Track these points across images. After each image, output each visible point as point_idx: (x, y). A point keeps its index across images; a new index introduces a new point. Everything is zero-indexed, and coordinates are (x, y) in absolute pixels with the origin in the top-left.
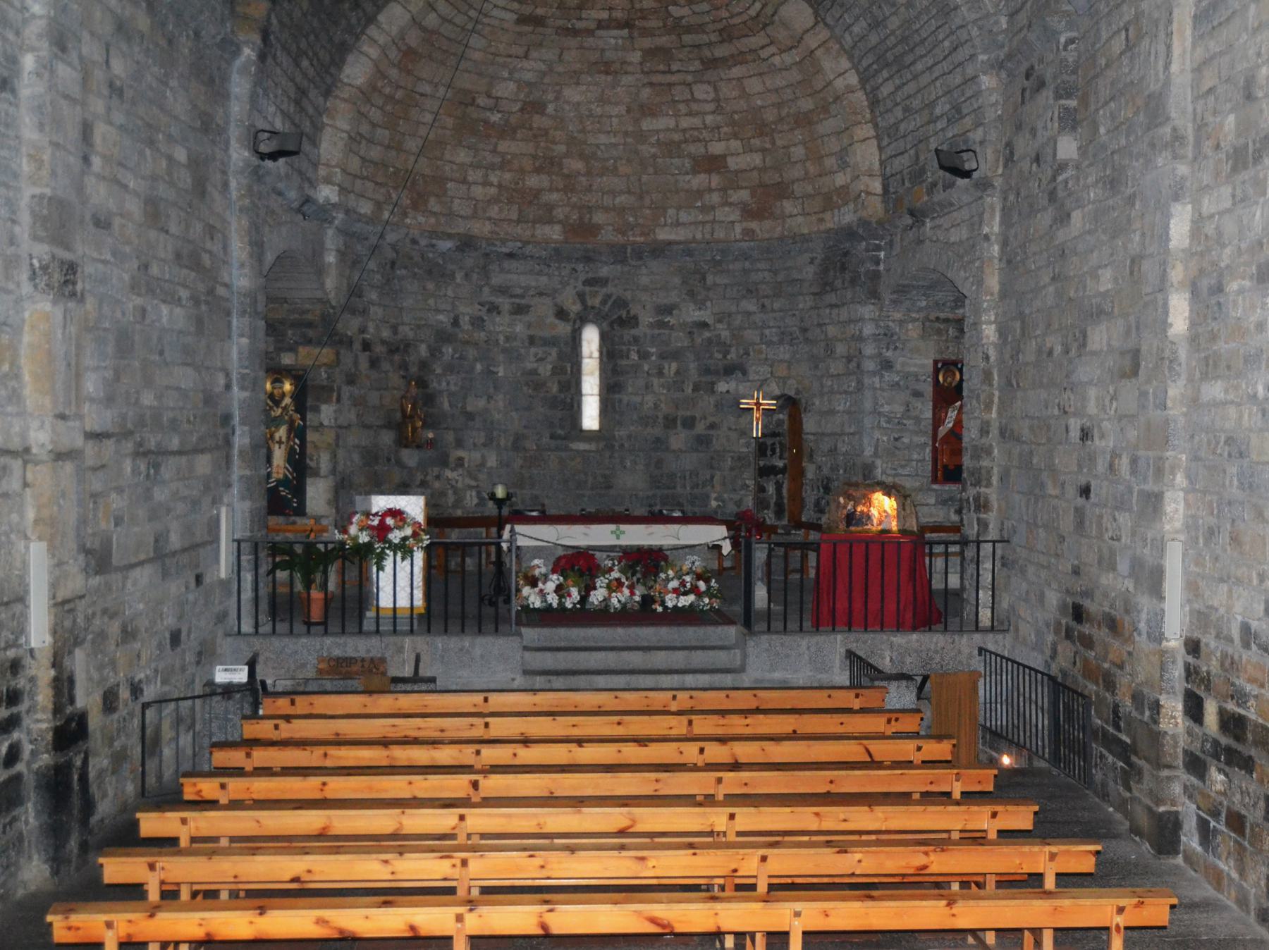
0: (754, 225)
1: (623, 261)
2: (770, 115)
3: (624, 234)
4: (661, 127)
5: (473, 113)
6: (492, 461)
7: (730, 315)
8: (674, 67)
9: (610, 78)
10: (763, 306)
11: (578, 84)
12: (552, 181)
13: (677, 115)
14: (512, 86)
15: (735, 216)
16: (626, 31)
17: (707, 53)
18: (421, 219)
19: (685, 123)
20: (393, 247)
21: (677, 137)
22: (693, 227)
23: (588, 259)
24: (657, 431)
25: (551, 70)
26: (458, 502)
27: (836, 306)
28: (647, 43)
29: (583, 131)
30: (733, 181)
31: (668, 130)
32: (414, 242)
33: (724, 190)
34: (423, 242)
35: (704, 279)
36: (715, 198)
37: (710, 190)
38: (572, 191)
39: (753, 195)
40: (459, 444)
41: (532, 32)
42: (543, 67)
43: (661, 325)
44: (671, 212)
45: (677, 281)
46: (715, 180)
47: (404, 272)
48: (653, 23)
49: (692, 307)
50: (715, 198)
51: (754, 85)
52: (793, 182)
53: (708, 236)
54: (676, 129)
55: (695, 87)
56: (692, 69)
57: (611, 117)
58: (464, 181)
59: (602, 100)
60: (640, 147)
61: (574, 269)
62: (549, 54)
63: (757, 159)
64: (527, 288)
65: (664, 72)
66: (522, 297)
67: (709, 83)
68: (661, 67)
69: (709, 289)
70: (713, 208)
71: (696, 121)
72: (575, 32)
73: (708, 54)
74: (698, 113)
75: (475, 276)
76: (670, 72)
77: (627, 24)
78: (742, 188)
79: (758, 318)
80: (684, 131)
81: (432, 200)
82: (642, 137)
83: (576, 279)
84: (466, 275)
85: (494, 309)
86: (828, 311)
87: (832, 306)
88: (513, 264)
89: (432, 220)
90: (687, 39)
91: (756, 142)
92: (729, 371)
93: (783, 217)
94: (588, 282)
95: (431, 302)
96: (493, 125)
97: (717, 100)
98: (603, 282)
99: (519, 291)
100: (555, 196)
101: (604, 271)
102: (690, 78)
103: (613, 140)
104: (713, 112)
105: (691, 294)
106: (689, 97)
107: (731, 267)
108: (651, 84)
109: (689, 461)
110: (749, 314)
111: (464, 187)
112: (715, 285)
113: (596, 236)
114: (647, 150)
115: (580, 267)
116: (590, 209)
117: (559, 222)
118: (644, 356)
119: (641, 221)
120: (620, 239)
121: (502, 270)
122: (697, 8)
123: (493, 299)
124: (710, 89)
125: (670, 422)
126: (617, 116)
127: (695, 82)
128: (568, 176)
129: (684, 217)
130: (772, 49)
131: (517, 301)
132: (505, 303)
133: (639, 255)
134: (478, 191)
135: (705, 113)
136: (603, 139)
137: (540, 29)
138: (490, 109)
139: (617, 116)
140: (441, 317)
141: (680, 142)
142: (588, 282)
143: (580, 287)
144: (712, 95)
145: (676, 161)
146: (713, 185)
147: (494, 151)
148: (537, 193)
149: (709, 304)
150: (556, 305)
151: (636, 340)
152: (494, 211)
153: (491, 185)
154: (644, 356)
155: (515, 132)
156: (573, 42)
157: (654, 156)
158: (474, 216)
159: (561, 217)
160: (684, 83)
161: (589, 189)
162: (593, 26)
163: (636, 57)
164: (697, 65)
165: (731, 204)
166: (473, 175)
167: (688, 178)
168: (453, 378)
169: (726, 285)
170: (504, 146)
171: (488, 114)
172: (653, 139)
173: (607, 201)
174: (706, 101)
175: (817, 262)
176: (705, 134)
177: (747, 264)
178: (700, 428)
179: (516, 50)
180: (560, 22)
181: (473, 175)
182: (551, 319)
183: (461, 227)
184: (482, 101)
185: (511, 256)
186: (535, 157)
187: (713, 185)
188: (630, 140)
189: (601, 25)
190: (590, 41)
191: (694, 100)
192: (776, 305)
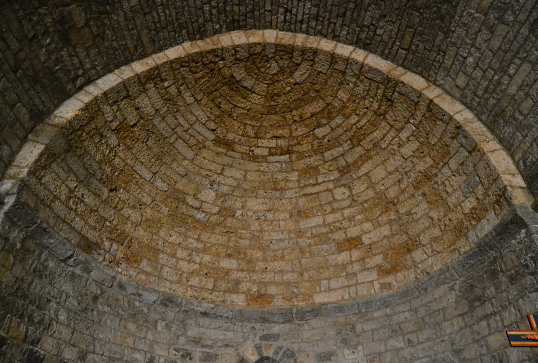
0: (389, 279)
1: (290, 321)
2: (391, 194)
3: (289, 300)
4: (313, 225)
5: (183, 209)
7: (380, 354)
8: (320, 180)
9: (278, 194)
10: (409, 341)
11: (256, 197)
12: (239, 264)
15: (374, 275)
16: (288, 156)
17: (342, 162)
18: (132, 273)
19: (330, 218)
20: (100, 284)
21: (324, 230)
22: (341, 291)
23: (264, 320)
25: (239, 185)
27: (494, 313)
28: (301, 164)
29: (261, 231)
31: (318, 226)
32: (121, 286)
34: (130, 290)
35: (354, 327)
36: (356, 267)
37: (352, 262)
38: (254, 271)
39: (385, 259)
41: (226, 155)
42: (235, 184)
44: (324, 282)
45: (332, 333)
46: (356, 254)
47: (106, 309)
48: (305, 147)
49: (347, 352)
50: (356, 267)
51: (379, 173)
52: (418, 235)
53: (353, 295)
54: (324, 225)
55: (335, 191)
56: (332, 178)
57: (279, 220)
58: (174, 255)
60: (300, 240)
61: (253, 327)
63: (386, 231)
64: (216, 341)
65: (314, 185)
66: (211, 347)
67: (344, 185)
68: (312, 181)
69: (358, 336)
70: (355, 274)
71: (337, 216)
72: (255, 158)
73: (344, 163)
74: (338, 209)
75: (174, 328)
76: (318, 184)
77: (289, 152)
78: (376, 255)
80: (329, 225)
81: (145, 262)
82: (300, 233)
83: (255, 335)
84: (167, 325)
86: (484, 323)
87: (487, 317)
88: (205, 321)
89: (143, 277)
90: (327, 155)
91: (384, 218)
93: (415, 265)
94: (265, 338)
95: (130, 341)
96: (198, 221)
97: (351, 196)
98: (276, 337)
99: (209, 343)
100: (241, 275)
101: (276, 329)
102: (331, 186)
103: (281, 236)
104: (349, 207)
105: (345, 341)
106: (332, 199)
107: (375, 315)
108: (305, 195)
110: (398, 350)
111: (174, 261)
112: (364, 331)
113: (269, 303)
114: (304, 242)
115: (258, 326)
116: (266, 284)
117: (244, 293)
119: (303, 290)
120: (286, 305)
121: (198, 325)
122: (333, 124)
123: (187, 347)
124: (346, 191)
126: (283, 220)
127: (335, 188)
128: (249, 262)
129: (334, 284)
130: (392, 133)
131: (207, 350)
133: (302, 315)
134: (184, 265)
135: (344, 208)
136: (275, 236)
137: (231, 153)
138: (197, 209)
139: (283, 220)
140: (138, 356)
141: (327, 233)
142: (265, 338)
143: (258, 341)
144: (348, 193)
145: (325, 246)
146: (354, 259)
147: (198, 240)
148: (227, 272)
149: (360, 348)
150: (238, 355)
152: (195, 281)
153: (194, 262)
155: (214, 229)
156: (253, 166)
157: (310, 245)
158: (179, 282)
159: (245, 289)
160: (328, 190)
162: (265, 152)
163: (294, 176)
164: (336, 174)
165: (368, 269)
166: (180, 253)
167: (334, 257)
169: (373, 331)
170: (205, 236)
171: (195, 212)
172: (308, 234)
173: (278, 278)
174: (343, 200)
175: (457, 287)
176: (345, 224)
177: (388, 311)
179: (213, 167)
180: (244, 149)
181: (180, 253)
183: (166, 288)
184: (190, 200)
185: (205, 314)
186: (227, 247)
187: (354, 259)
188: (292, 235)
190: (264, 166)
191: (335, 200)
192: (423, 337)
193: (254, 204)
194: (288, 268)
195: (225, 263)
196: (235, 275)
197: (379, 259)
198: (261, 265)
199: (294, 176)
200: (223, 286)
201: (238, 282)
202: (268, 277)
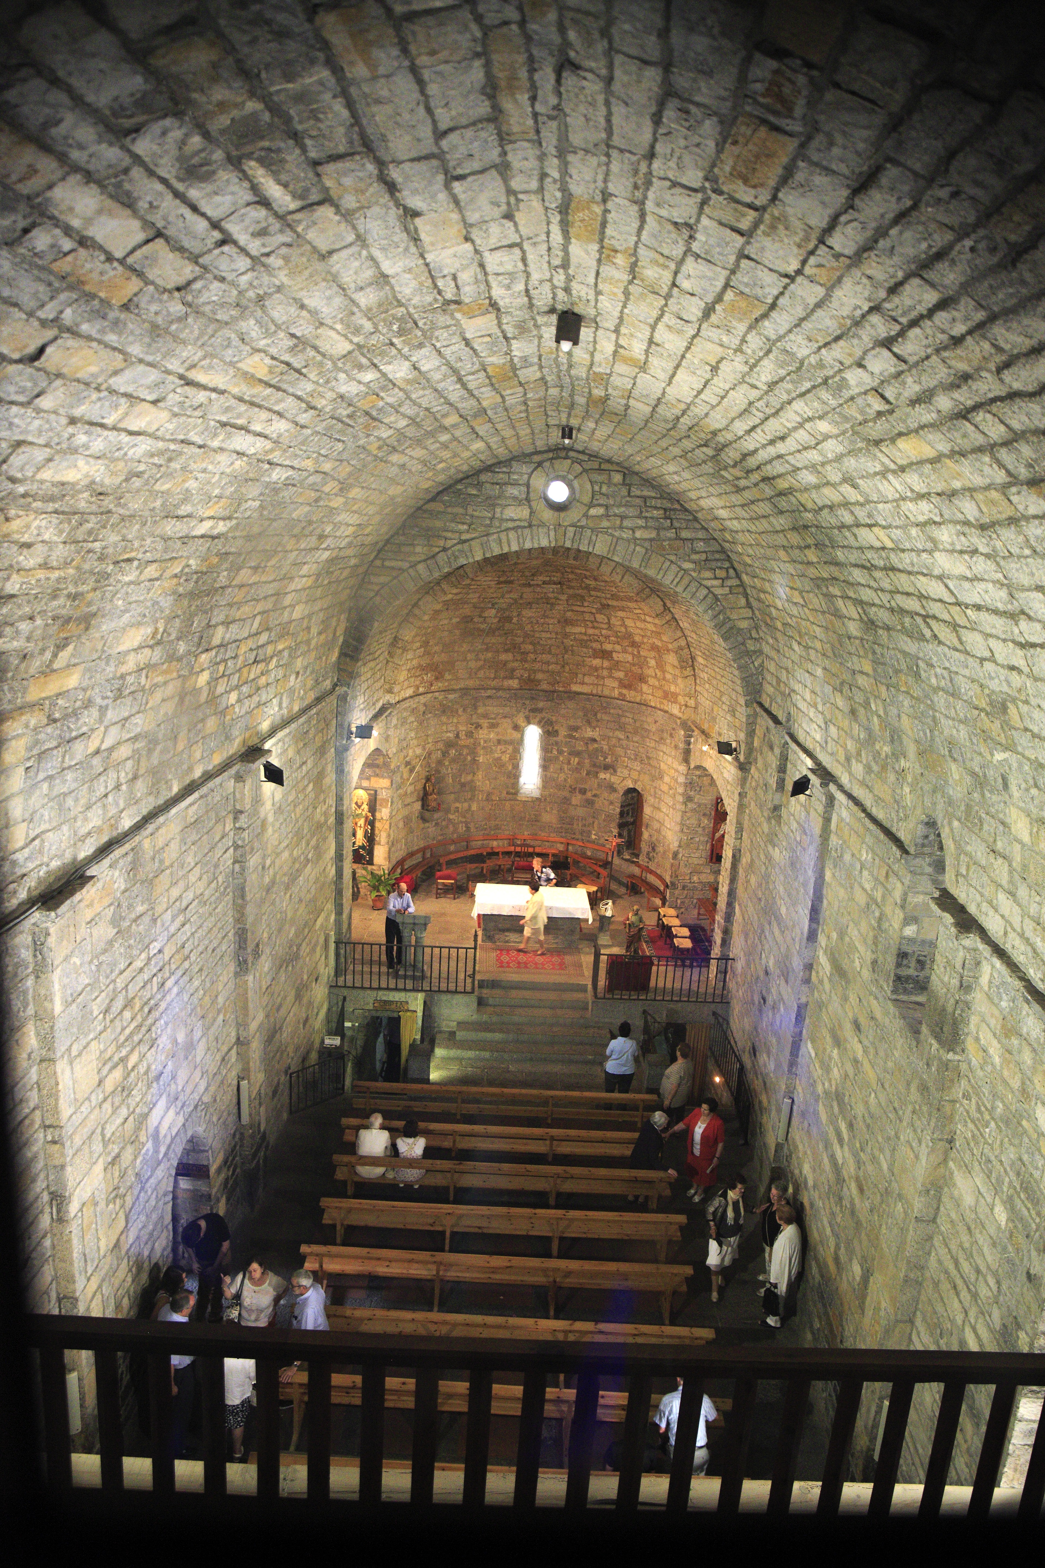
0: (625, 691)
6: (474, 807)
13: (586, 626)
14: (493, 611)
15: (616, 684)
24: (566, 793)
26: (455, 831)
30: (617, 665)
33: (610, 669)
36: (605, 673)
40: (457, 800)
43: (571, 736)
45: (581, 714)
46: (606, 664)
59: (545, 616)
62: (514, 595)
71: (597, 632)
79: (624, 743)
82: (566, 635)
85: (478, 726)
88: (490, 702)
92: (606, 768)
93: (642, 693)
100: (516, 664)
101: (541, 705)
105: (589, 722)
109: (581, 812)
116: (535, 671)
118: (560, 752)
125: (573, 790)
129: (587, 679)
132: (485, 723)
136: (544, 635)
148: (505, 663)
151: (557, 743)
152: (481, 674)
154: (560, 752)
161: (535, 660)
166: (469, 656)
168: (454, 766)
170: (487, 640)
173: (545, 667)
178: (589, 795)
182: (510, 731)
189: (544, 583)
193: (527, 613)
194: (554, 660)
195: (503, 657)
196: (510, 665)
197: (621, 675)
198: (532, 656)
199: (564, 597)
200: (502, 674)
201: (513, 670)
202: (537, 666)
